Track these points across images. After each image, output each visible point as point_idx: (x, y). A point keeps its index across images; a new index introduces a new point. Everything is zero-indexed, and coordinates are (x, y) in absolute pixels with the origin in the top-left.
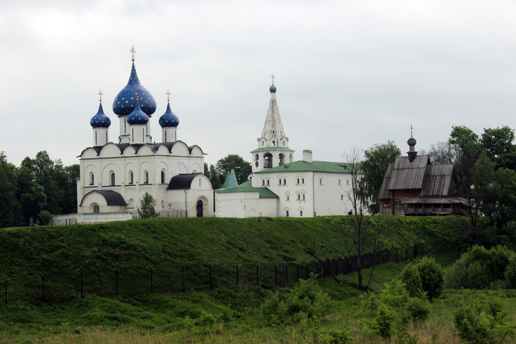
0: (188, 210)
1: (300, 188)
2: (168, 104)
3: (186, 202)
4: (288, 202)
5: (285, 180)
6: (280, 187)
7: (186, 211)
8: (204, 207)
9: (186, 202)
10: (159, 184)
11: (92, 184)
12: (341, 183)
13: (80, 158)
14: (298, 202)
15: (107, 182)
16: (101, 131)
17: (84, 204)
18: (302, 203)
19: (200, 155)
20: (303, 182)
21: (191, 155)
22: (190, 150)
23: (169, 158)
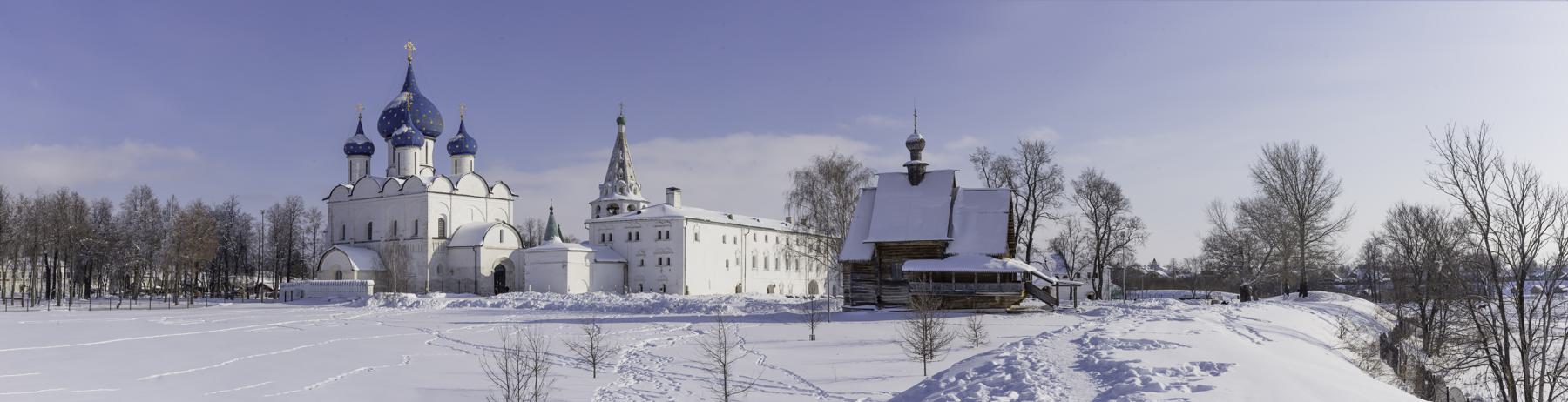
0: (478, 279)
1: (663, 243)
2: (462, 122)
3: (476, 267)
4: (642, 268)
5: (638, 234)
6: (629, 243)
7: (476, 283)
8: (507, 275)
9: (476, 267)
10: (434, 238)
11: (344, 239)
12: (726, 241)
13: (328, 201)
14: (659, 268)
15: (363, 236)
16: (359, 161)
17: (322, 268)
18: (666, 269)
19: (506, 196)
20: (668, 237)
21: (491, 196)
22: (489, 189)
23: (453, 197)
